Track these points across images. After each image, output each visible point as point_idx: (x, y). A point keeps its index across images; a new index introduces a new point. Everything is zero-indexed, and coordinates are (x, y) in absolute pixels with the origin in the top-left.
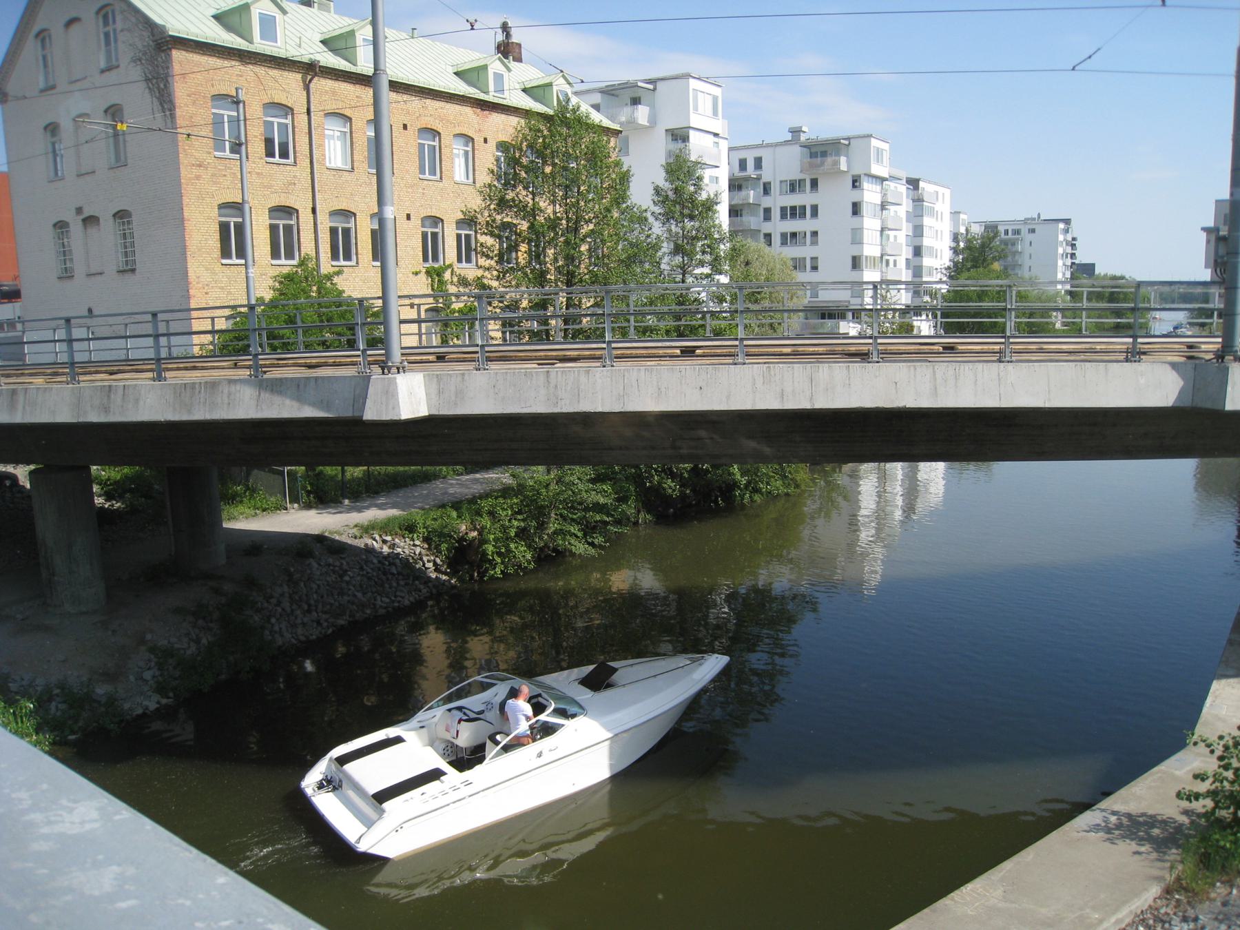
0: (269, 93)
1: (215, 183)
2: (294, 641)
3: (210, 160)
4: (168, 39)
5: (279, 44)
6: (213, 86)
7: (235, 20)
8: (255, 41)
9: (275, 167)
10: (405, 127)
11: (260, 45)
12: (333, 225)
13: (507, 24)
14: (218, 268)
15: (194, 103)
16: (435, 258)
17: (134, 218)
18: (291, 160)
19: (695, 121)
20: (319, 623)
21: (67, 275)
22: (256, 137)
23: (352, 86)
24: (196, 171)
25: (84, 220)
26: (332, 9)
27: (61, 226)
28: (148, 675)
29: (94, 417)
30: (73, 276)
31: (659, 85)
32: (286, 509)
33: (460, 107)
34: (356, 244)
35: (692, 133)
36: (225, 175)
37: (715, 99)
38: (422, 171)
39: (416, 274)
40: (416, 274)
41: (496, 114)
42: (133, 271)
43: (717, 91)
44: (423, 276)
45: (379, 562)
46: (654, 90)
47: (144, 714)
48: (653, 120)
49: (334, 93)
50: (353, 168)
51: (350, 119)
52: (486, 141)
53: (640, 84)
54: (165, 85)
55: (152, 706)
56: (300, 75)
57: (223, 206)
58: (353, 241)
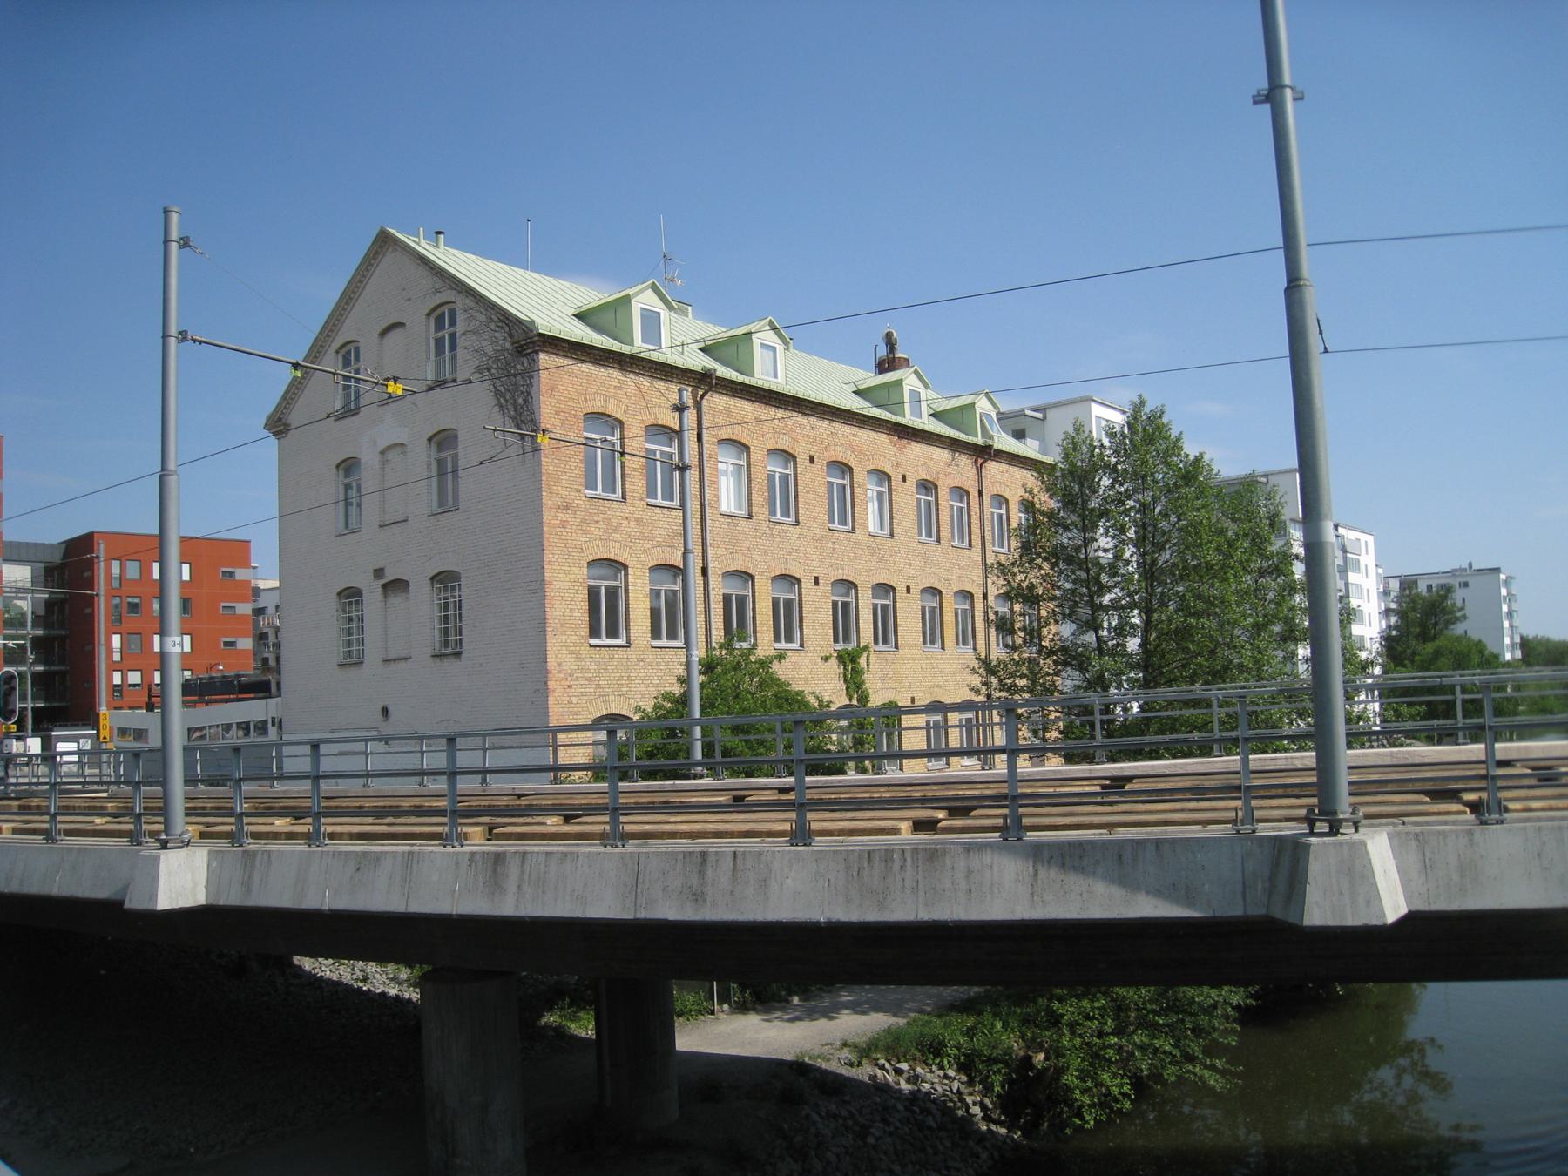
0: (652, 410)
1: (585, 532)
3: (579, 500)
4: (537, 338)
6: (586, 400)
7: (608, 318)
9: (658, 511)
10: (812, 460)
12: (728, 591)
14: (585, 651)
16: (847, 639)
17: (463, 582)
21: (353, 661)
22: (635, 469)
23: (750, 404)
25: (385, 586)
26: (690, 315)
27: (351, 596)
29: (671, 910)
30: (362, 663)
32: (712, 1013)
34: (754, 618)
36: (597, 522)
38: (832, 521)
39: (826, 659)
40: (826, 659)
41: (915, 444)
42: (458, 655)
44: (833, 662)
45: (906, 1108)
49: (729, 412)
50: (750, 514)
51: (747, 448)
52: (904, 479)
53: (1028, 412)
54: (526, 401)
57: (593, 563)
58: (750, 614)
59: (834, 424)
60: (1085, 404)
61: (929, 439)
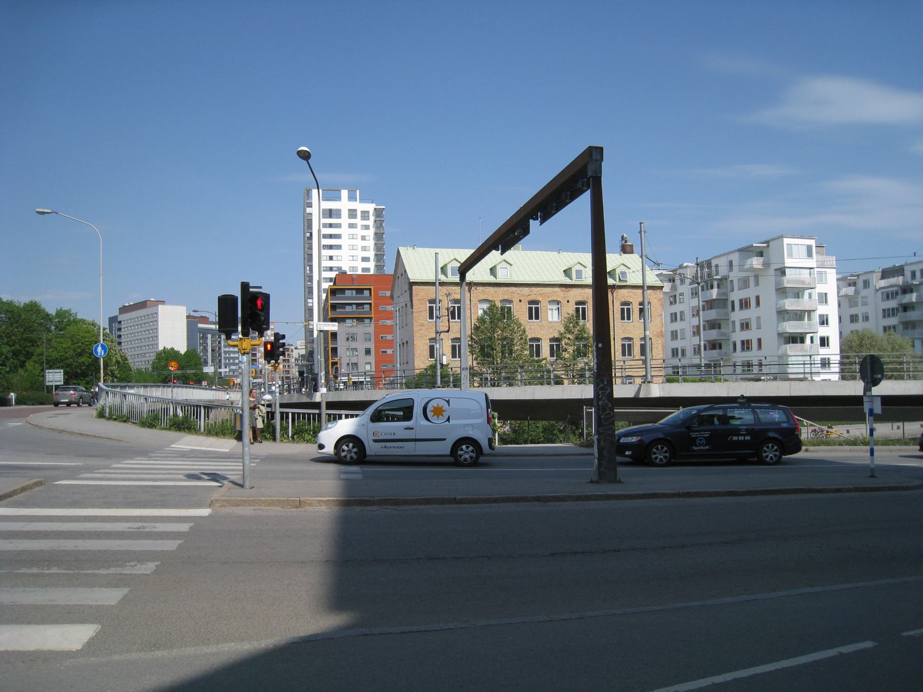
8: (448, 277)
10: (520, 301)
13: (624, 236)
15: (420, 303)
19: (788, 262)
24: (420, 328)
31: (771, 243)
35: (787, 270)
37: (809, 248)
43: (812, 242)
46: (768, 246)
48: (766, 265)
49: (484, 292)
52: (568, 301)
53: (754, 245)
57: (430, 339)
60: (781, 239)
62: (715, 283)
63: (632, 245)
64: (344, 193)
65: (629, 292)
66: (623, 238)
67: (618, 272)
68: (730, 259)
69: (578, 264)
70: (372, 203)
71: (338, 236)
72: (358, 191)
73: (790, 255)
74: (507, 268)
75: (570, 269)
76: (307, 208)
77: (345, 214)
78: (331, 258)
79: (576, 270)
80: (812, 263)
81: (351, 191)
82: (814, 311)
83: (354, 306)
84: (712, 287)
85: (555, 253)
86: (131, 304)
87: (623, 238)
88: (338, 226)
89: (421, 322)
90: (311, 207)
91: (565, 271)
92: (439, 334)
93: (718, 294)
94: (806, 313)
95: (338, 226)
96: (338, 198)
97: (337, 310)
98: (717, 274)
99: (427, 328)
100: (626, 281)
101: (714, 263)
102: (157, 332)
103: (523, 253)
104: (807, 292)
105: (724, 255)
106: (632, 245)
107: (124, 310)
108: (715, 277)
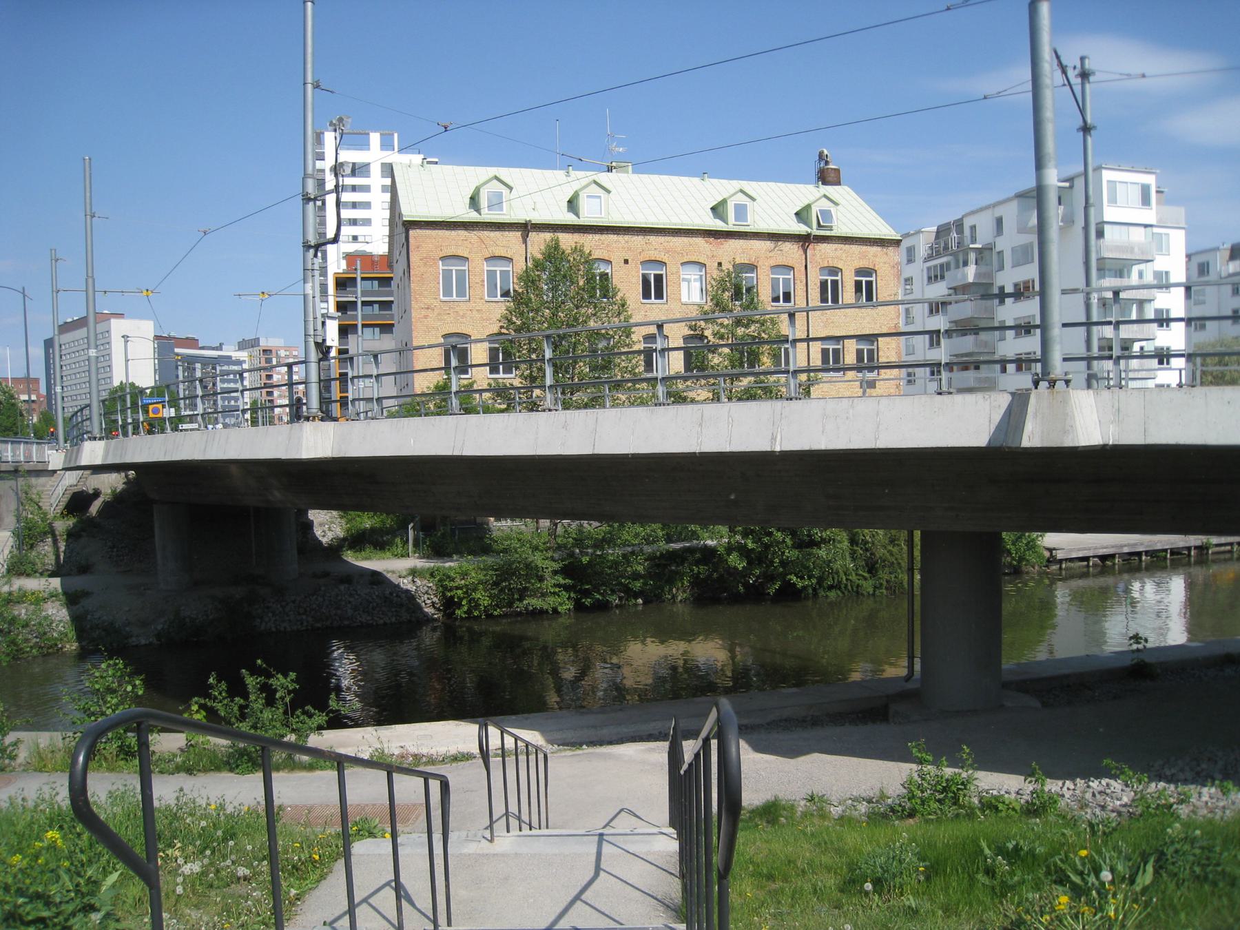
2: (274, 629)
5: (504, 212)
6: (441, 250)
9: (494, 304)
10: (626, 262)
11: (487, 216)
13: (823, 152)
18: (467, 298)
20: (302, 624)
22: (477, 283)
23: (570, 234)
24: (424, 312)
28: (159, 627)
33: (689, 239)
35: (1107, 228)
37: (1145, 190)
41: (733, 240)
43: (1150, 180)
46: (1071, 187)
47: (137, 646)
55: (143, 642)
56: (520, 233)
59: (648, 237)
61: (746, 236)
62: (972, 256)
63: (837, 171)
64: (375, 138)
65: (836, 250)
66: (821, 155)
67: (815, 210)
68: (997, 215)
69: (740, 194)
70: (419, 153)
71: (367, 205)
72: (396, 135)
73: (1113, 200)
74: (600, 197)
75: (723, 202)
76: (317, 162)
77: (376, 170)
78: (355, 238)
79: (735, 204)
80: (1149, 216)
81: (386, 134)
82: (1150, 301)
83: (376, 306)
84: (966, 264)
85: (696, 180)
86: (75, 318)
87: (821, 155)
88: (366, 189)
89: (426, 301)
90: (323, 160)
91: (713, 209)
92: (312, 251)
93: (977, 275)
94: (1135, 305)
95: (366, 189)
96: (364, 145)
97: (349, 313)
98: (974, 241)
99: (439, 314)
100: (830, 229)
101: (968, 223)
102: (110, 359)
103: (635, 177)
104: (1135, 269)
105: (987, 207)
106: (837, 171)
107: (66, 328)
108: (971, 246)
